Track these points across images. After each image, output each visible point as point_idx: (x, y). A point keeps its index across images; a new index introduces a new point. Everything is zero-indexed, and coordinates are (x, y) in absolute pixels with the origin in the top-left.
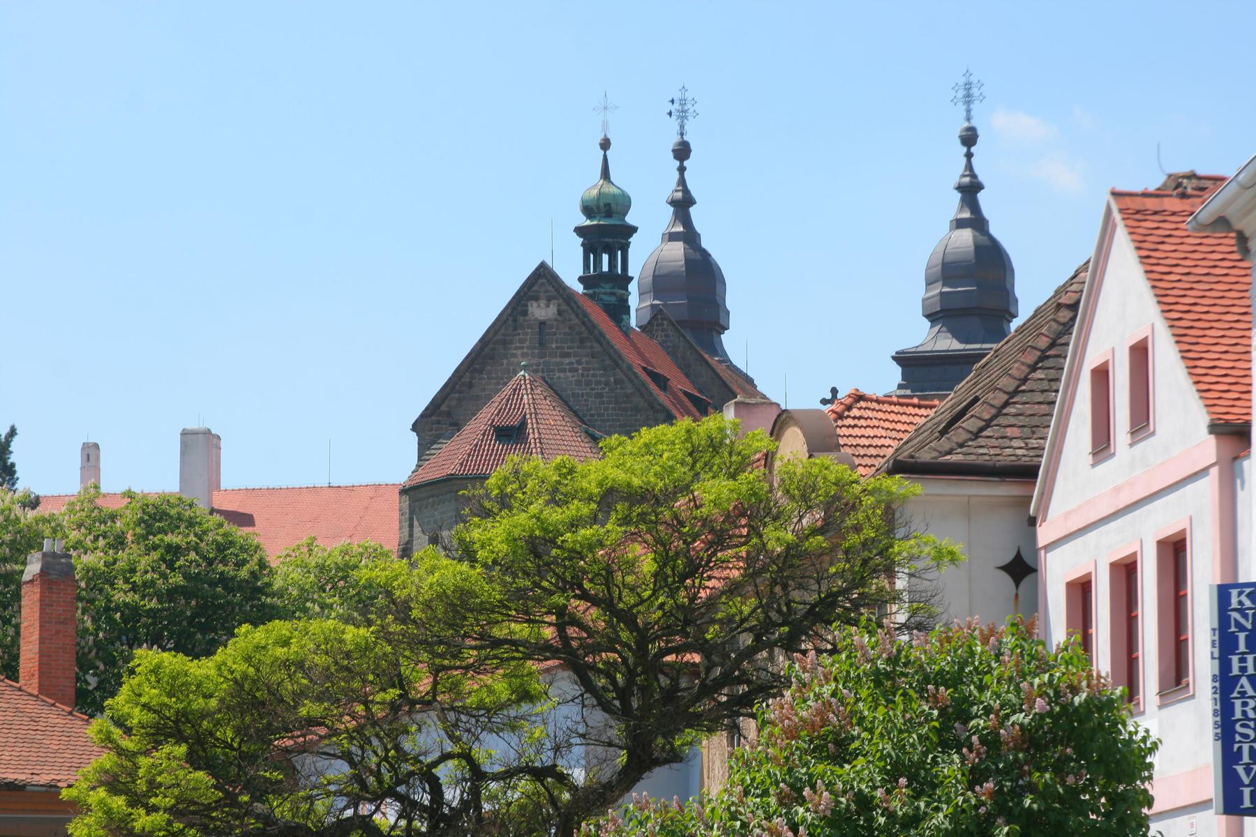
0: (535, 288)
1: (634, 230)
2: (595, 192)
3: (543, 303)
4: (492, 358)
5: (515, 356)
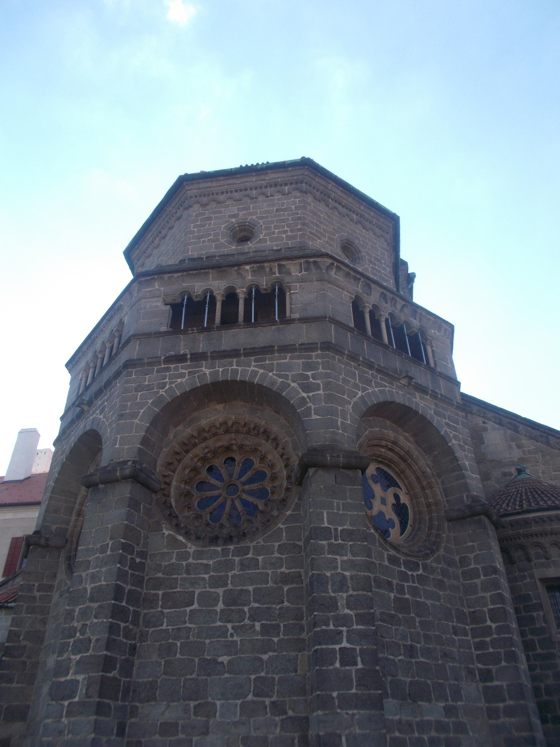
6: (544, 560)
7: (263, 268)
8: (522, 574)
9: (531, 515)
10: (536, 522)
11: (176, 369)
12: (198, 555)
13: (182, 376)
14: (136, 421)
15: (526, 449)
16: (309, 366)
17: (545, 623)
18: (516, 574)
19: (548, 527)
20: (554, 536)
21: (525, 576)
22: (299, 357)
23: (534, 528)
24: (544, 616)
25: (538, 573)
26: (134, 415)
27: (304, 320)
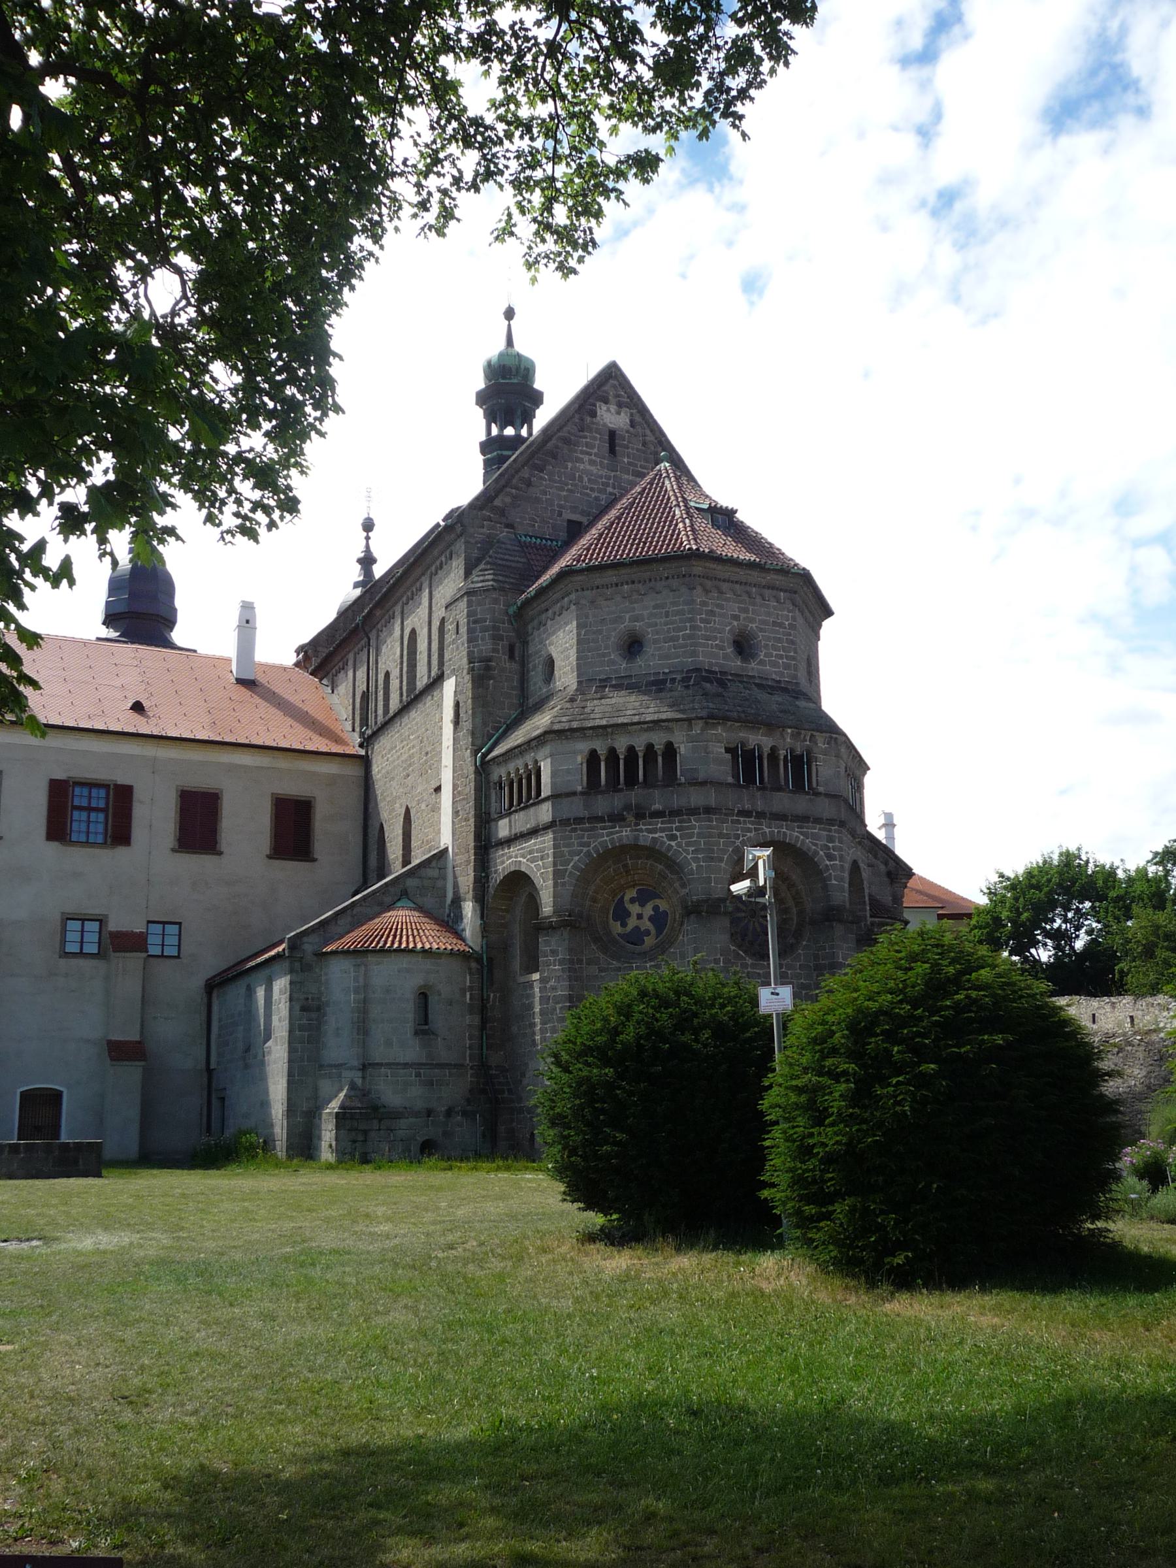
0: (605, 388)
1: (611, 385)
2: (501, 355)
3: (613, 408)
4: (555, 457)
5: (581, 461)
7: (799, 734)
11: (745, 822)
12: (753, 966)
13: (749, 830)
14: (723, 865)
16: (831, 839)
22: (824, 830)
26: (721, 860)
27: (827, 795)
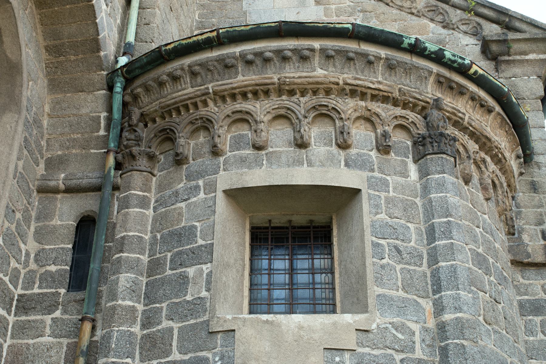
6: (248, 152)
8: (194, 183)
9: (237, 49)
10: (249, 63)
15: (333, 7)
17: (208, 290)
18: (182, 185)
19: (273, 76)
20: (284, 97)
21: (197, 187)
23: (240, 77)
24: (210, 274)
25: (226, 179)
